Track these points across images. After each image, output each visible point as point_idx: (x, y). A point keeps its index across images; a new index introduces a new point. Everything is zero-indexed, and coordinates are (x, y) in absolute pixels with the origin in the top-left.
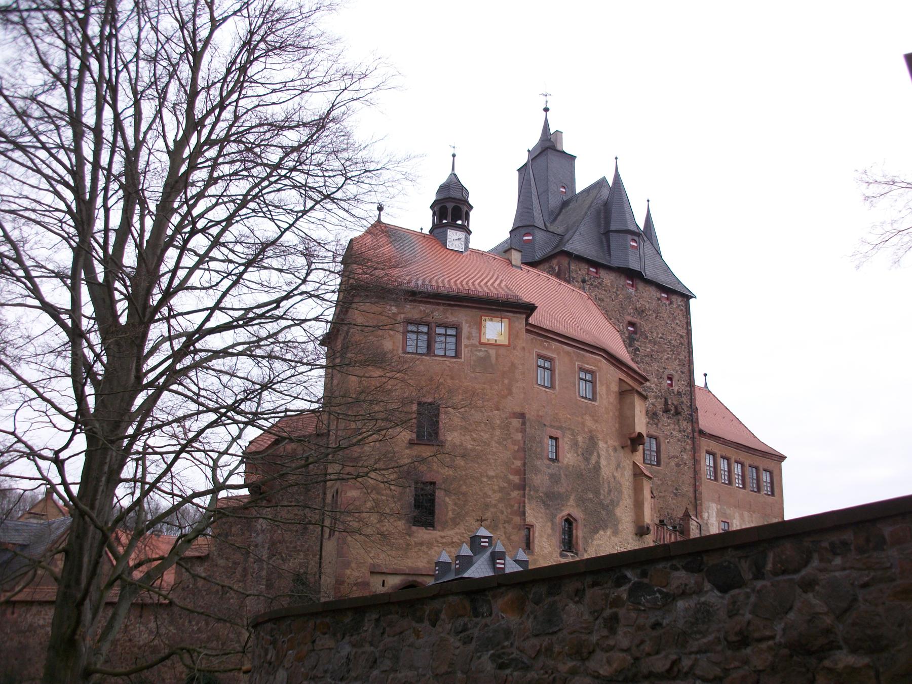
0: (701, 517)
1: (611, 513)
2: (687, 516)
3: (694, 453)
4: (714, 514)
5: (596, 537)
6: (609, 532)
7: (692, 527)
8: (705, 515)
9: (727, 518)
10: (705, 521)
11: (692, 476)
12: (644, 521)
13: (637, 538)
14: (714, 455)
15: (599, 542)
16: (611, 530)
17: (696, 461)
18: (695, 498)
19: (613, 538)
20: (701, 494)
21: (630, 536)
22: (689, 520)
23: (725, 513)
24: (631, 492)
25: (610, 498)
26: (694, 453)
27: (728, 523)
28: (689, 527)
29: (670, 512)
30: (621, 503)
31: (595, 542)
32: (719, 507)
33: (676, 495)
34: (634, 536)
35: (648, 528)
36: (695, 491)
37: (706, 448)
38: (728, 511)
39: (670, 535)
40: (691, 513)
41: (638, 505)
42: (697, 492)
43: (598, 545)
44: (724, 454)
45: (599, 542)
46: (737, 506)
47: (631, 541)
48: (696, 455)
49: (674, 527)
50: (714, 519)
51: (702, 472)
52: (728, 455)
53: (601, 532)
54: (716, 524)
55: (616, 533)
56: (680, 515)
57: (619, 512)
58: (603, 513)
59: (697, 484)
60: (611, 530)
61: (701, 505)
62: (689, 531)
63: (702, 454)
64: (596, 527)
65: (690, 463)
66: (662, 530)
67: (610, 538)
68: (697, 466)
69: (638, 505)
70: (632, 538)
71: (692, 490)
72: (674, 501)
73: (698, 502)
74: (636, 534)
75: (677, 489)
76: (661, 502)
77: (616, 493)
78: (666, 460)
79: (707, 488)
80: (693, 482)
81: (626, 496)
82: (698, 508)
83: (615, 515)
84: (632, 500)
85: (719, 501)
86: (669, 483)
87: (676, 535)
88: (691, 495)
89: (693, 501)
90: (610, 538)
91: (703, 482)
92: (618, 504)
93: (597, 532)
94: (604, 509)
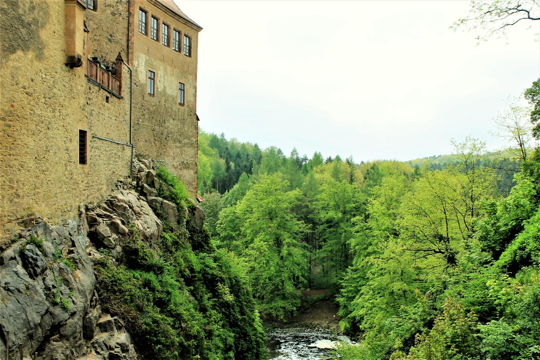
0: (132, 64)
1: (33, 35)
2: (119, 60)
3: (129, 7)
4: (143, 63)
5: (12, 57)
6: (31, 55)
7: (123, 70)
8: (136, 63)
9: (154, 69)
10: (135, 68)
11: (126, 26)
12: (74, 52)
13: (67, 69)
14: (146, 12)
15: (17, 64)
16: (34, 54)
17: (130, 14)
18: (128, 46)
19: (36, 63)
20: (133, 44)
21: (59, 65)
22: (121, 64)
23: (152, 64)
24: (62, 19)
25: (32, 16)
26: (129, 7)
27: (154, 73)
28: (121, 70)
29: (104, 55)
30: (48, 26)
31: (11, 63)
32: (148, 58)
33: (110, 40)
34: (64, 67)
35: (79, 60)
36: (128, 40)
37: (140, 5)
38: (155, 63)
39: (103, 74)
40: (124, 58)
41: (69, 34)
42: (130, 42)
43: (17, 68)
44: (154, 14)
45: (16, 64)
46: (163, 60)
47: (59, 70)
48: (131, 8)
49: (107, 68)
50: (143, 68)
51: (135, 25)
52: (158, 16)
53: (20, 53)
54: (144, 72)
55: (40, 57)
56: (113, 59)
57: (44, 34)
58: (24, 31)
59: (130, 34)
60: (34, 54)
61: (132, 53)
62: (121, 73)
63: (136, 9)
64: (12, 46)
65: (125, 15)
66: (94, 67)
67: (32, 61)
68: (130, 19)
69: (69, 34)
70: (61, 68)
71: (125, 39)
72: (108, 46)
73: (130, 51)
74: (66, 65)
75: (111, 36)
76: (96, 45)
77: (41, 13)
78: (103, 7)
79: (138, 39)
80: (127, 32)
81: (55, 21)
82: (130, 55)
83: (39, 37)
84: (63, 26)
85: (148, 53)
86: (105, 29)
87: (109, 75)
88: (124, 42)
89: (125, 48)
90: (32, 61)
91: (135, 34)
92: (43, 26)
93: (14, 51)
94: (23, 27)
